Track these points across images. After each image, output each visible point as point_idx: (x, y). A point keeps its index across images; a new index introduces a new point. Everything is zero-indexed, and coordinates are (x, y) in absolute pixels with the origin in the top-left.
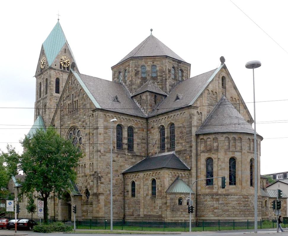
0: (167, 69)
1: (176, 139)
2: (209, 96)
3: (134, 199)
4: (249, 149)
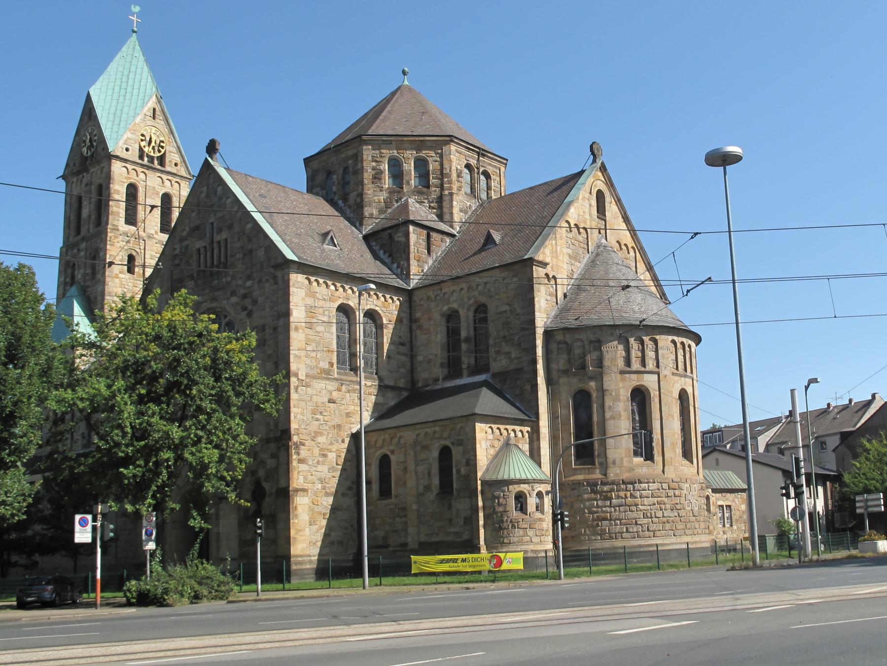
0: (454, 168)
1: (491, 342)
2: (570, 235)
3: (390, 501)
4: (675, 367)
